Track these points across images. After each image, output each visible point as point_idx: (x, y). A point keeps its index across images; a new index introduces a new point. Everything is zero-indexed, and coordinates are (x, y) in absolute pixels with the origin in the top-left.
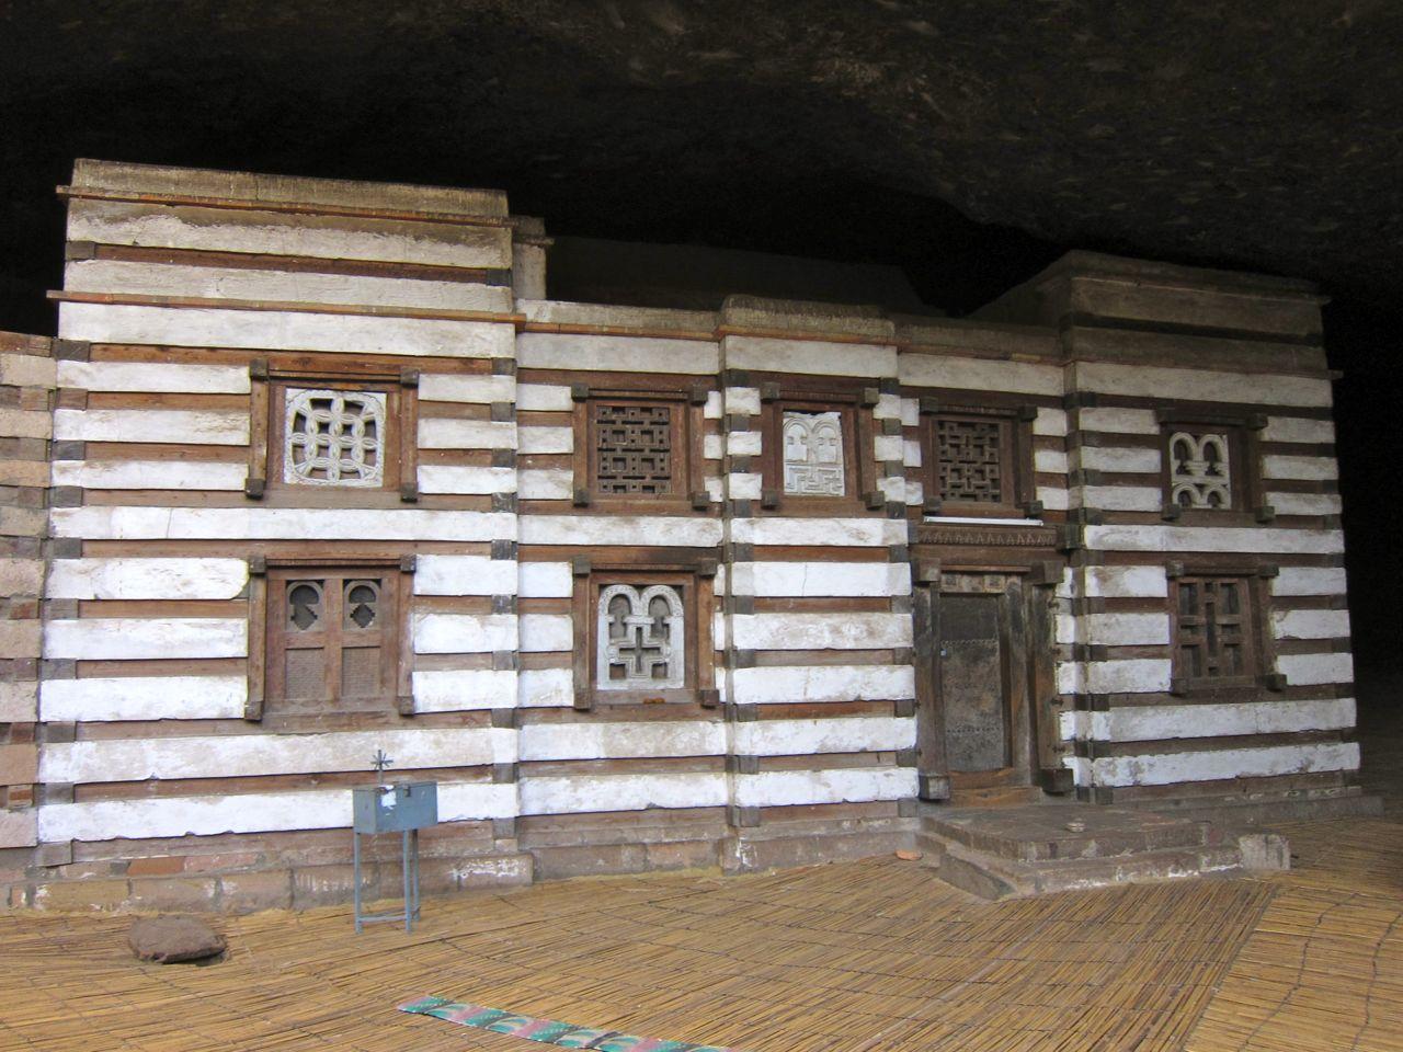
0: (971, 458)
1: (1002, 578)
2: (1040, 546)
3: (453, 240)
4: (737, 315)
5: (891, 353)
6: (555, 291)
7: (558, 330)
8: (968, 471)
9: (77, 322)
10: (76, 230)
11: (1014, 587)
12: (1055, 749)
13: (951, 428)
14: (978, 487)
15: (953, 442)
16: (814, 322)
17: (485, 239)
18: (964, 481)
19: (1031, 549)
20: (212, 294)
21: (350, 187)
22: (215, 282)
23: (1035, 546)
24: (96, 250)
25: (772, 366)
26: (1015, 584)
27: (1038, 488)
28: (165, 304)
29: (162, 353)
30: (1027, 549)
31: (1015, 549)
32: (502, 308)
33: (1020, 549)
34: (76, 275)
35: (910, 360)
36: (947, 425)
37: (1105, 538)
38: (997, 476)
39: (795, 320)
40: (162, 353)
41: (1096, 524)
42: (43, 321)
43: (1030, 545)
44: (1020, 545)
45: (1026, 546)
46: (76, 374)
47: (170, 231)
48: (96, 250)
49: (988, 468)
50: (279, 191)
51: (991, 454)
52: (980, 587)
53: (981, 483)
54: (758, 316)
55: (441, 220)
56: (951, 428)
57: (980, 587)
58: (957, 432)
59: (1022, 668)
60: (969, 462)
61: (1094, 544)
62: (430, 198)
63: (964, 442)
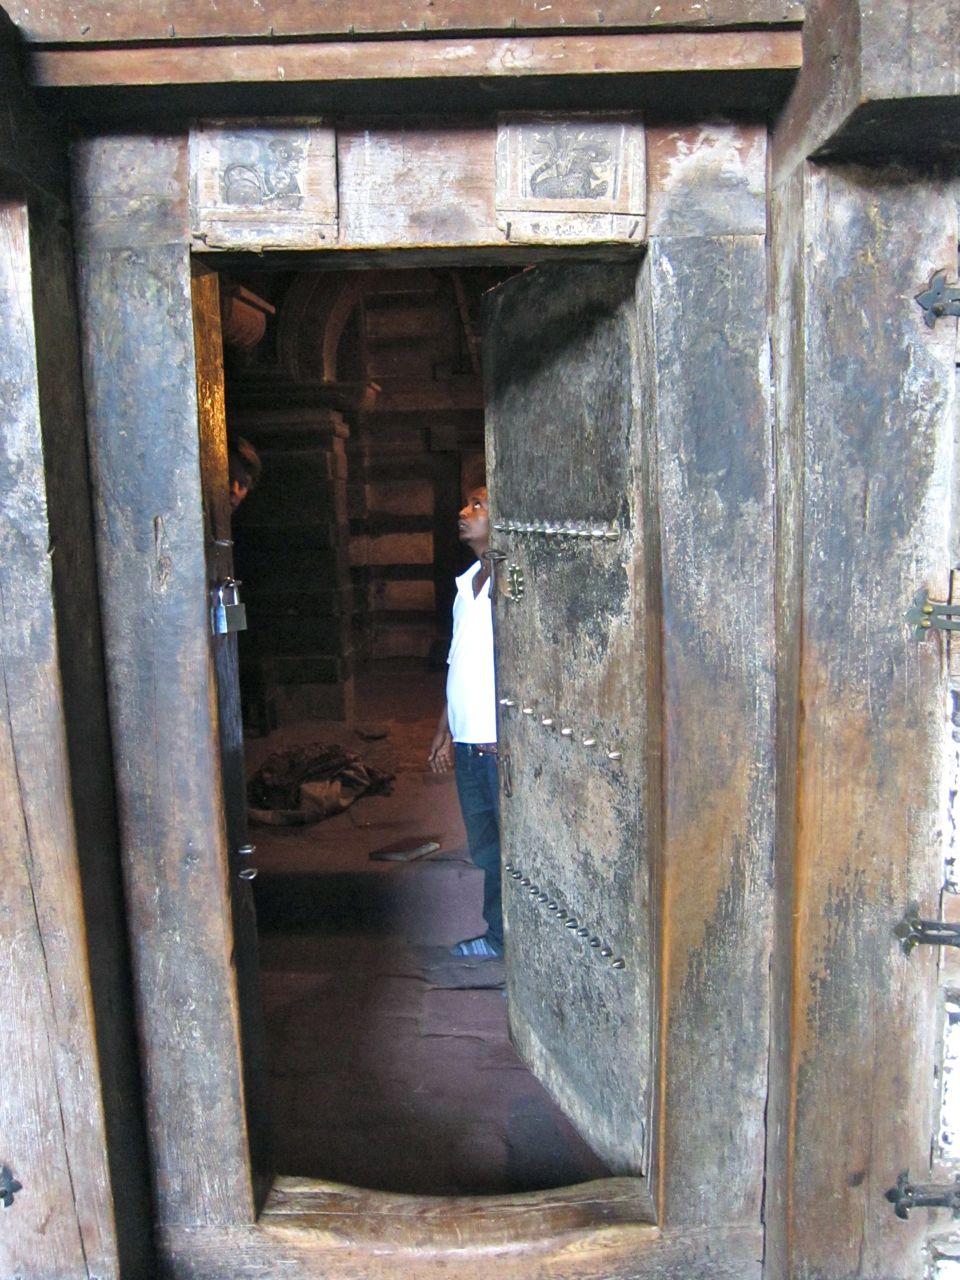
1: (628, 144)
11: (719, 206)
12: (900, 1199)
26: (718, 182)
52: (473, 209)
57: (473, 209)
59: (747, 704)
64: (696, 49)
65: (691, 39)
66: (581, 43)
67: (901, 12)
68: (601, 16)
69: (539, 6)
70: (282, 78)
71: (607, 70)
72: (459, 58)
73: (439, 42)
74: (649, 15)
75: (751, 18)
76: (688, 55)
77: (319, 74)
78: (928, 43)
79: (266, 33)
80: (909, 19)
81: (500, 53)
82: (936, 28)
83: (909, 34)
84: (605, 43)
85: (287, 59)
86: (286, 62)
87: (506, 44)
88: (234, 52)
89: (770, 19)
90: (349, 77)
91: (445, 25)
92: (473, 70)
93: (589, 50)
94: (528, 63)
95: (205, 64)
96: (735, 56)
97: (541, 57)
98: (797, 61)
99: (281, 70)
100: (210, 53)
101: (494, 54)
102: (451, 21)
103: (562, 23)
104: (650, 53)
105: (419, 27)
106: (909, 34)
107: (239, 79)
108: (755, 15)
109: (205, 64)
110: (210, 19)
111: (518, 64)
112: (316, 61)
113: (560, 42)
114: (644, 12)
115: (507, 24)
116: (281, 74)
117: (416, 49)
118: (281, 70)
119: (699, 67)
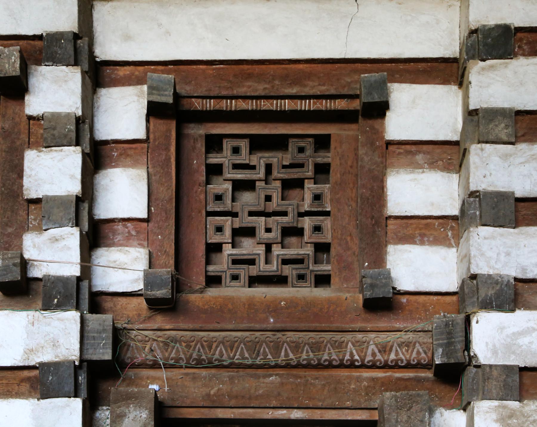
0: (274, 205)
2: (396, 366)
8: (268, 230)
13: (236, 150)
14: (285, 262)
15: (240, 175)
18: (261, 250)
19: (379, 374)
23: (386, 366)
27: (391, 248)
30: (367, 374)
31: (344, 373)
33: (355, 373)
36: (227, 145)
37: (524, 341)
38: (327, 237)
41: (500, 308)
43: (373, 366)
44: (352, 365)
45: (363, 366)
49: (307, 223)
51: (317, 197)
53: (291, 252)
56: (236, 150)
58: (244, 158)
60: (267, 215)
61: (495, 352)
63: (262, 174)
64: (348, 414)
65: (347, 411)
66: (316, 411)
67: (395, 416)
68: (322, 404)
69: (305, 401)
70: (232, 418)
71: (324, 419)
72: (282, 414)
73: (277, 409)
74: (335, 405)
75: (363, 406)
76: (346, 415)
77: (243, 417)
78: (402, 424)
79: (230, 406)
80: (397, 419)
81: (294, 413)
82: (404, 420)
83: (397, 421)
84: (323, 411)
85: (234, 412)
86: (233, 413)
87: (295, 410)
88: (219, 410)
89: (369, 407)
90: (251, 418)
91: (279, 405)
92: (286, 417)
93: (319, 413)
94: (302, 416)
95: (211, 413)
96: (359, 416)
97: (305, 414)
98: (377, 418)
99: (232, 415)
100: (212, 410)
101: (292, 413)
102: (280, 404)
103: (311, 406)
104: (336, 414)
105: (272, 406)
106: (397, 421)
107: (221, 418)
108: (364, 406)
109: (211, 413)
110: (214, 401)
111: (298, 416)
112: (242, 413)
113: (310, 411)
114: (334, 404)
115: (296, 406)
116: (232, 416)
117: (271, 412)
118: (232, 415)
119: (350, 418)
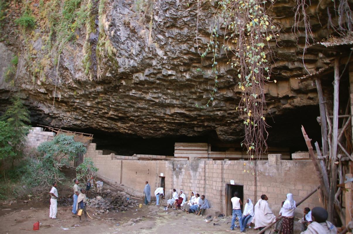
3: (203, 147)
4: (227, 152)
5: (241, 155)
6: (211, 151)
7: (212, 154)
9: (175, 155)
10: (175, 148)
16: (234, 153)
17: (206, 147)
20: (185, 153)
21: (195, 143)
22: (185, 152)
24: (176, 150)
25: (230, 157)
28: (182, 153)
29: (181, 157)
32: (207, 153)
34: (175, 151)
35: (243, 155)
39: (232, 153)
40: (181, 157)
42: (174, 155)
46: (175, 159)
47: (182, 148)
48: (176, 150)
50: (190, 144)
54: (229, 152)
55: (202, 146)
62: (201, 144)
